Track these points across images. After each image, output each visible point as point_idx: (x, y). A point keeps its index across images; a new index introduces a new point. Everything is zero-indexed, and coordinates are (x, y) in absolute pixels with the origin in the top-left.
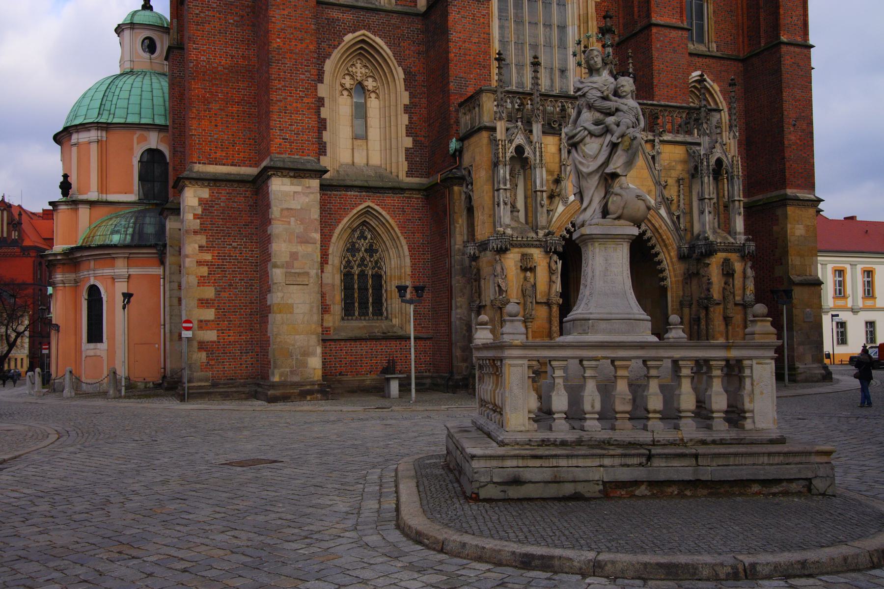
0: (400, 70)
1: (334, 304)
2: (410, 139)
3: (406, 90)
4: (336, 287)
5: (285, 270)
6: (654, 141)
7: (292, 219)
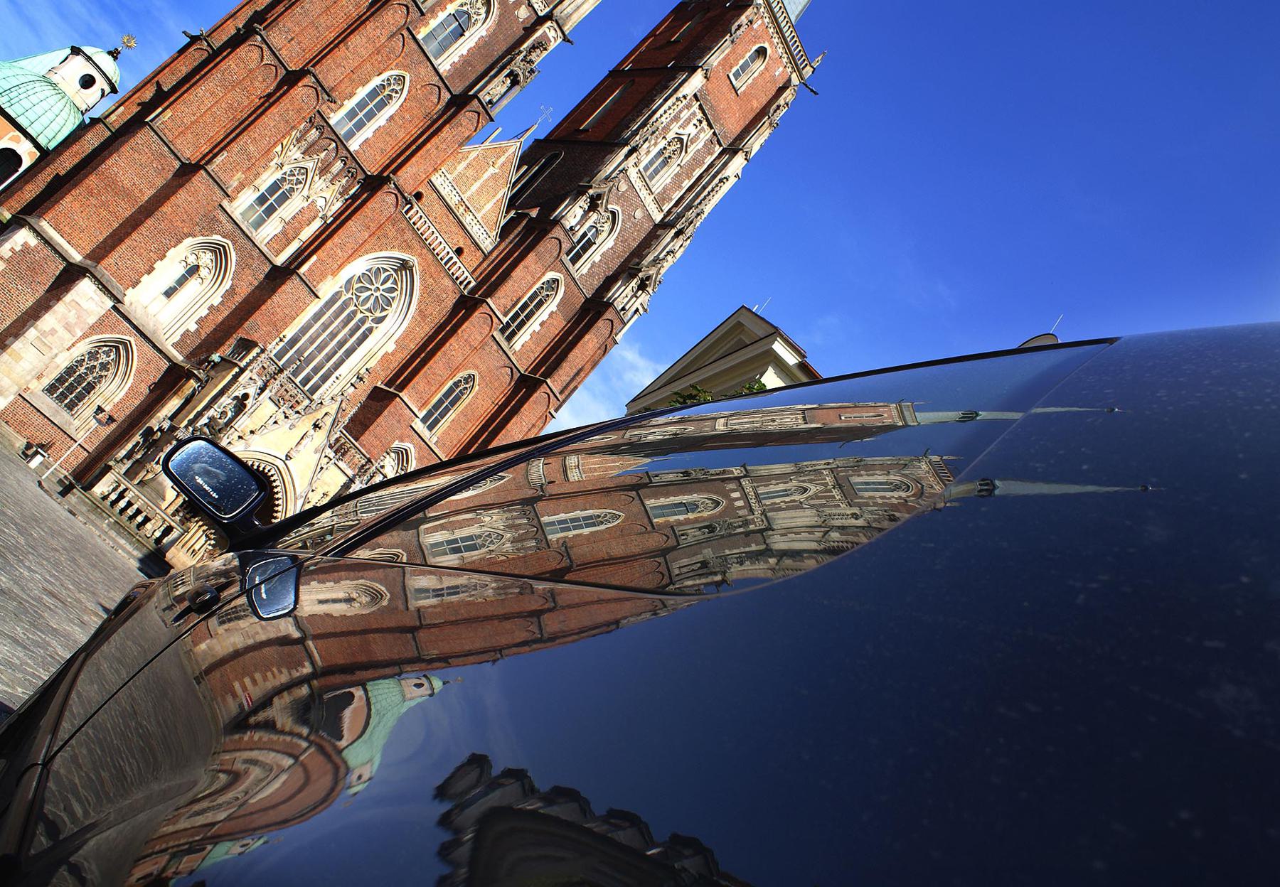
0: (230, 283)
1: (47, 377)
2: (197, 326)
3: (222, 297)
4: (59, 369)
5: (39, 335)
6: (331, 460)
7: (74, 311)
